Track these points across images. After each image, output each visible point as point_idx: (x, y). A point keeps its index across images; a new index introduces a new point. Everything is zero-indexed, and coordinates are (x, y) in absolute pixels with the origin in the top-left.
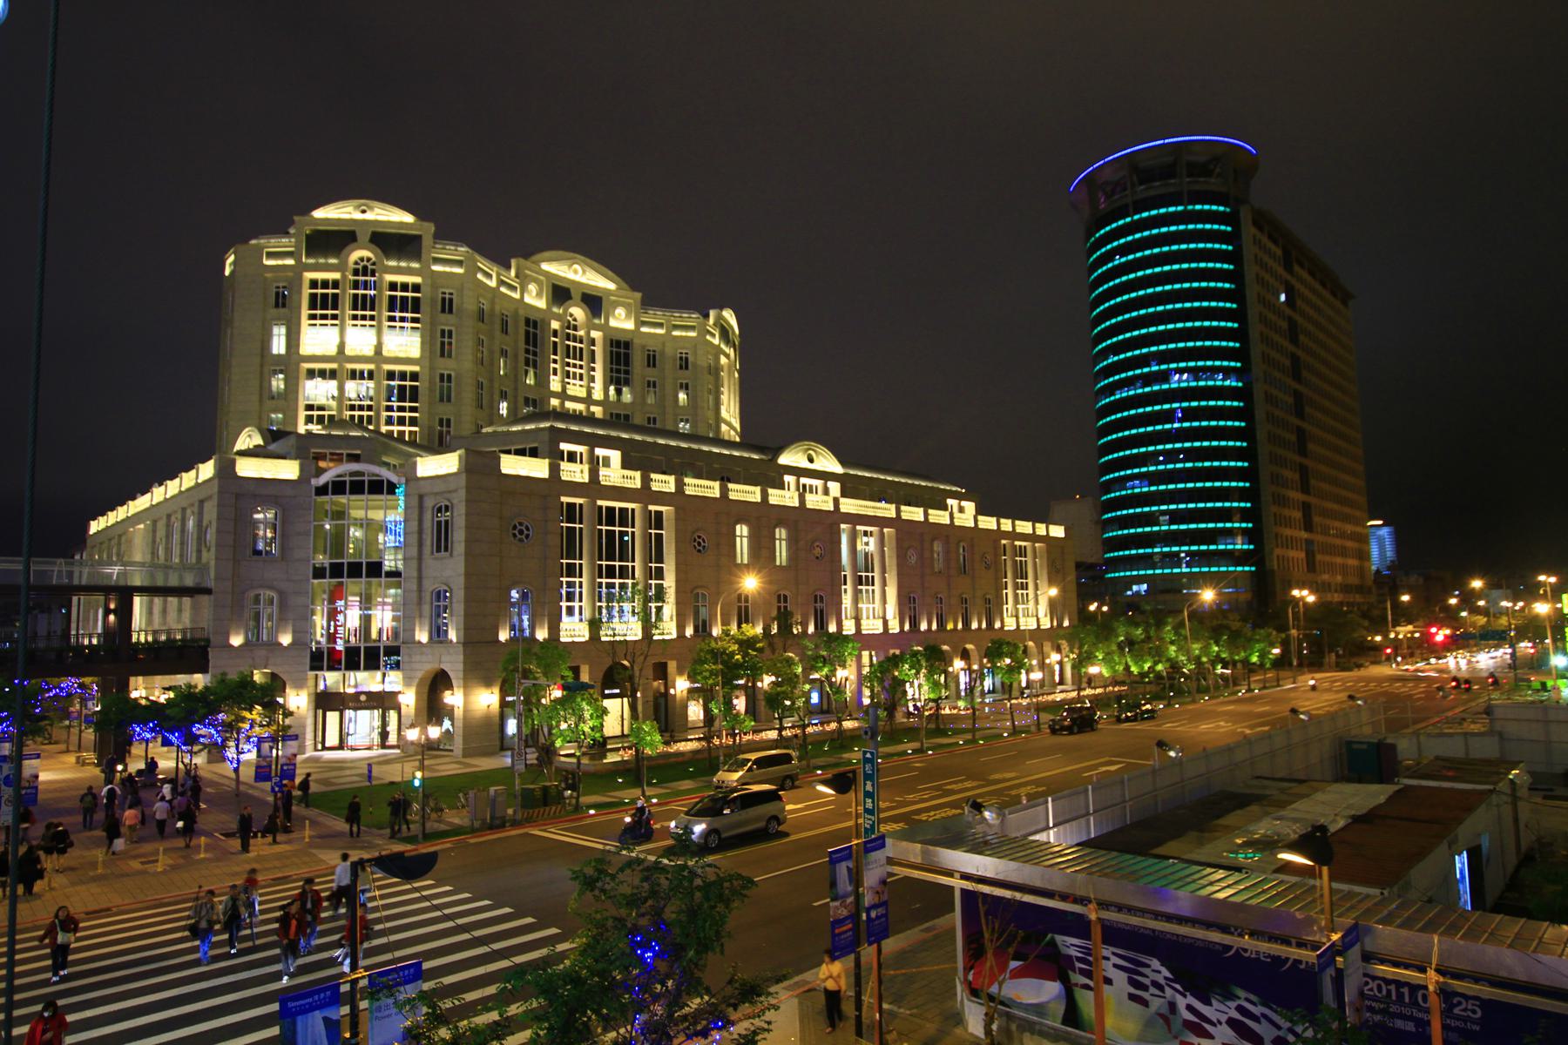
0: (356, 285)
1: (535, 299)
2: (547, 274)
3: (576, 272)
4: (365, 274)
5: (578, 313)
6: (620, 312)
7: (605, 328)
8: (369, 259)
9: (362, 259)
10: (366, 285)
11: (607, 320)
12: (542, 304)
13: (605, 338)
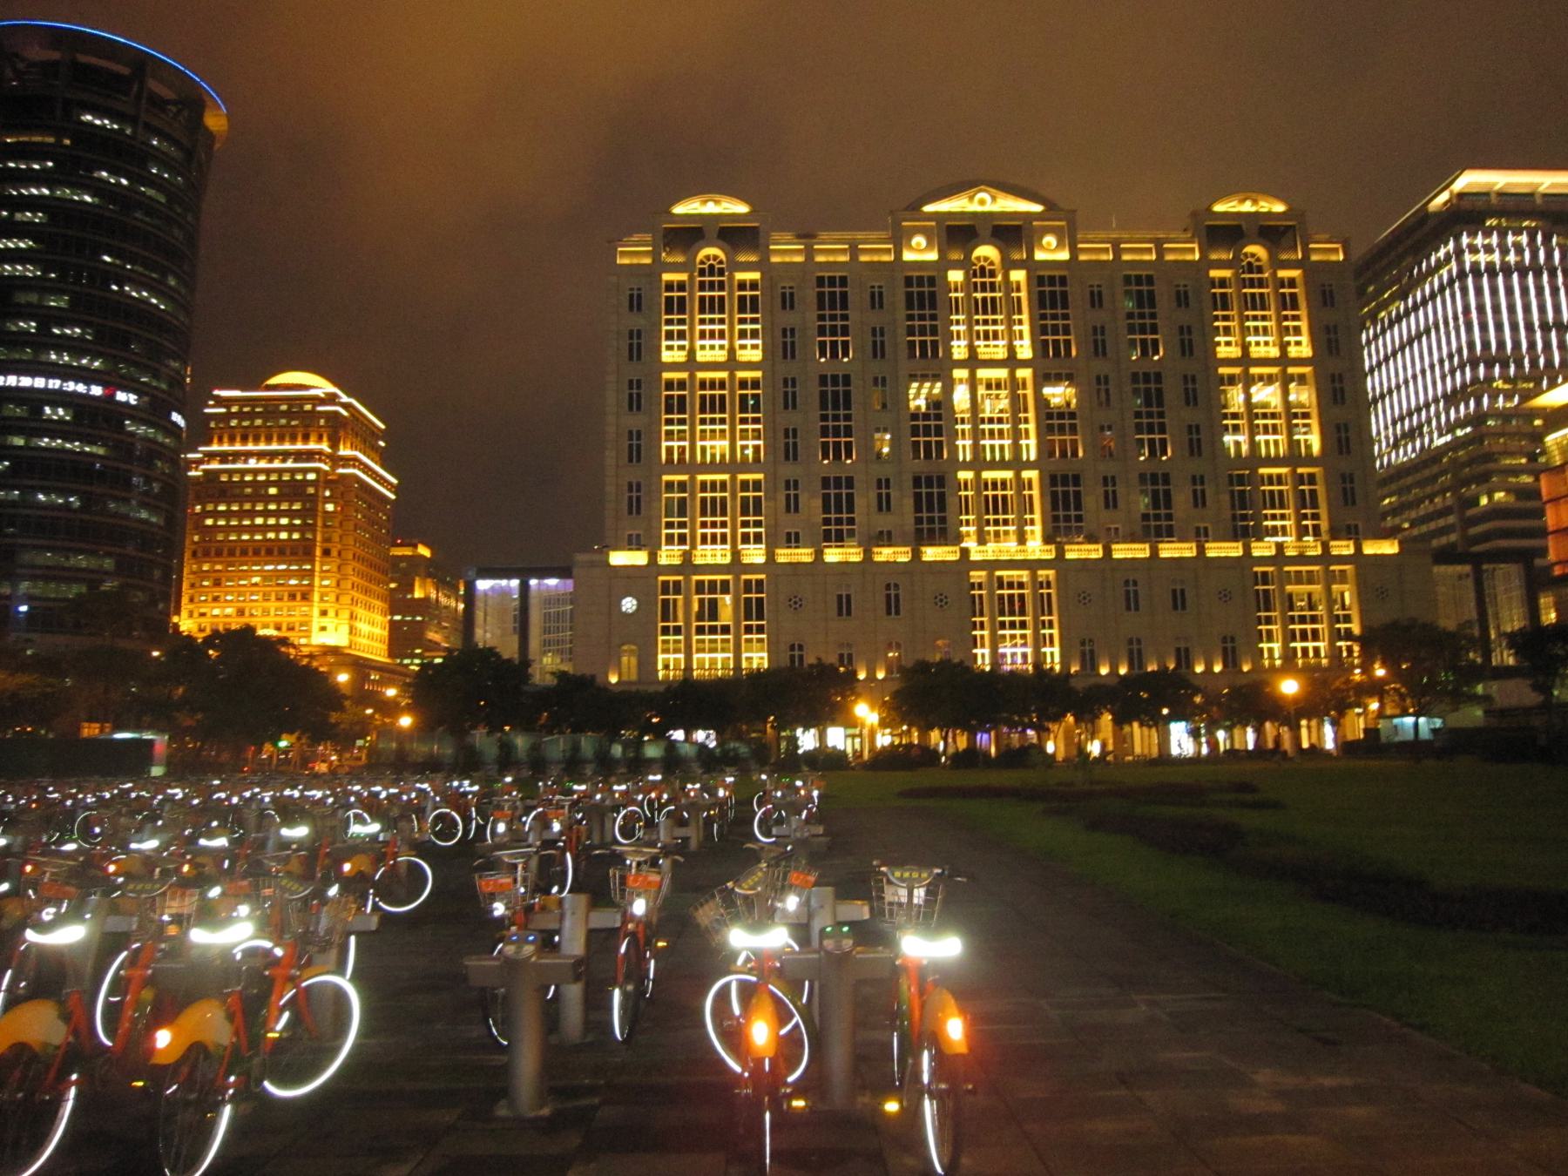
0: (702, 287)
1: (920, 251)
3: (982, 202)
4: (712, 274)
5: (987, 252)
6: (1050, 240)
8: (715, 258)
9: (708, 258)
10: (712, 286)
11: (1031, 253)
12: (933, 256)
13: (1029, 278)
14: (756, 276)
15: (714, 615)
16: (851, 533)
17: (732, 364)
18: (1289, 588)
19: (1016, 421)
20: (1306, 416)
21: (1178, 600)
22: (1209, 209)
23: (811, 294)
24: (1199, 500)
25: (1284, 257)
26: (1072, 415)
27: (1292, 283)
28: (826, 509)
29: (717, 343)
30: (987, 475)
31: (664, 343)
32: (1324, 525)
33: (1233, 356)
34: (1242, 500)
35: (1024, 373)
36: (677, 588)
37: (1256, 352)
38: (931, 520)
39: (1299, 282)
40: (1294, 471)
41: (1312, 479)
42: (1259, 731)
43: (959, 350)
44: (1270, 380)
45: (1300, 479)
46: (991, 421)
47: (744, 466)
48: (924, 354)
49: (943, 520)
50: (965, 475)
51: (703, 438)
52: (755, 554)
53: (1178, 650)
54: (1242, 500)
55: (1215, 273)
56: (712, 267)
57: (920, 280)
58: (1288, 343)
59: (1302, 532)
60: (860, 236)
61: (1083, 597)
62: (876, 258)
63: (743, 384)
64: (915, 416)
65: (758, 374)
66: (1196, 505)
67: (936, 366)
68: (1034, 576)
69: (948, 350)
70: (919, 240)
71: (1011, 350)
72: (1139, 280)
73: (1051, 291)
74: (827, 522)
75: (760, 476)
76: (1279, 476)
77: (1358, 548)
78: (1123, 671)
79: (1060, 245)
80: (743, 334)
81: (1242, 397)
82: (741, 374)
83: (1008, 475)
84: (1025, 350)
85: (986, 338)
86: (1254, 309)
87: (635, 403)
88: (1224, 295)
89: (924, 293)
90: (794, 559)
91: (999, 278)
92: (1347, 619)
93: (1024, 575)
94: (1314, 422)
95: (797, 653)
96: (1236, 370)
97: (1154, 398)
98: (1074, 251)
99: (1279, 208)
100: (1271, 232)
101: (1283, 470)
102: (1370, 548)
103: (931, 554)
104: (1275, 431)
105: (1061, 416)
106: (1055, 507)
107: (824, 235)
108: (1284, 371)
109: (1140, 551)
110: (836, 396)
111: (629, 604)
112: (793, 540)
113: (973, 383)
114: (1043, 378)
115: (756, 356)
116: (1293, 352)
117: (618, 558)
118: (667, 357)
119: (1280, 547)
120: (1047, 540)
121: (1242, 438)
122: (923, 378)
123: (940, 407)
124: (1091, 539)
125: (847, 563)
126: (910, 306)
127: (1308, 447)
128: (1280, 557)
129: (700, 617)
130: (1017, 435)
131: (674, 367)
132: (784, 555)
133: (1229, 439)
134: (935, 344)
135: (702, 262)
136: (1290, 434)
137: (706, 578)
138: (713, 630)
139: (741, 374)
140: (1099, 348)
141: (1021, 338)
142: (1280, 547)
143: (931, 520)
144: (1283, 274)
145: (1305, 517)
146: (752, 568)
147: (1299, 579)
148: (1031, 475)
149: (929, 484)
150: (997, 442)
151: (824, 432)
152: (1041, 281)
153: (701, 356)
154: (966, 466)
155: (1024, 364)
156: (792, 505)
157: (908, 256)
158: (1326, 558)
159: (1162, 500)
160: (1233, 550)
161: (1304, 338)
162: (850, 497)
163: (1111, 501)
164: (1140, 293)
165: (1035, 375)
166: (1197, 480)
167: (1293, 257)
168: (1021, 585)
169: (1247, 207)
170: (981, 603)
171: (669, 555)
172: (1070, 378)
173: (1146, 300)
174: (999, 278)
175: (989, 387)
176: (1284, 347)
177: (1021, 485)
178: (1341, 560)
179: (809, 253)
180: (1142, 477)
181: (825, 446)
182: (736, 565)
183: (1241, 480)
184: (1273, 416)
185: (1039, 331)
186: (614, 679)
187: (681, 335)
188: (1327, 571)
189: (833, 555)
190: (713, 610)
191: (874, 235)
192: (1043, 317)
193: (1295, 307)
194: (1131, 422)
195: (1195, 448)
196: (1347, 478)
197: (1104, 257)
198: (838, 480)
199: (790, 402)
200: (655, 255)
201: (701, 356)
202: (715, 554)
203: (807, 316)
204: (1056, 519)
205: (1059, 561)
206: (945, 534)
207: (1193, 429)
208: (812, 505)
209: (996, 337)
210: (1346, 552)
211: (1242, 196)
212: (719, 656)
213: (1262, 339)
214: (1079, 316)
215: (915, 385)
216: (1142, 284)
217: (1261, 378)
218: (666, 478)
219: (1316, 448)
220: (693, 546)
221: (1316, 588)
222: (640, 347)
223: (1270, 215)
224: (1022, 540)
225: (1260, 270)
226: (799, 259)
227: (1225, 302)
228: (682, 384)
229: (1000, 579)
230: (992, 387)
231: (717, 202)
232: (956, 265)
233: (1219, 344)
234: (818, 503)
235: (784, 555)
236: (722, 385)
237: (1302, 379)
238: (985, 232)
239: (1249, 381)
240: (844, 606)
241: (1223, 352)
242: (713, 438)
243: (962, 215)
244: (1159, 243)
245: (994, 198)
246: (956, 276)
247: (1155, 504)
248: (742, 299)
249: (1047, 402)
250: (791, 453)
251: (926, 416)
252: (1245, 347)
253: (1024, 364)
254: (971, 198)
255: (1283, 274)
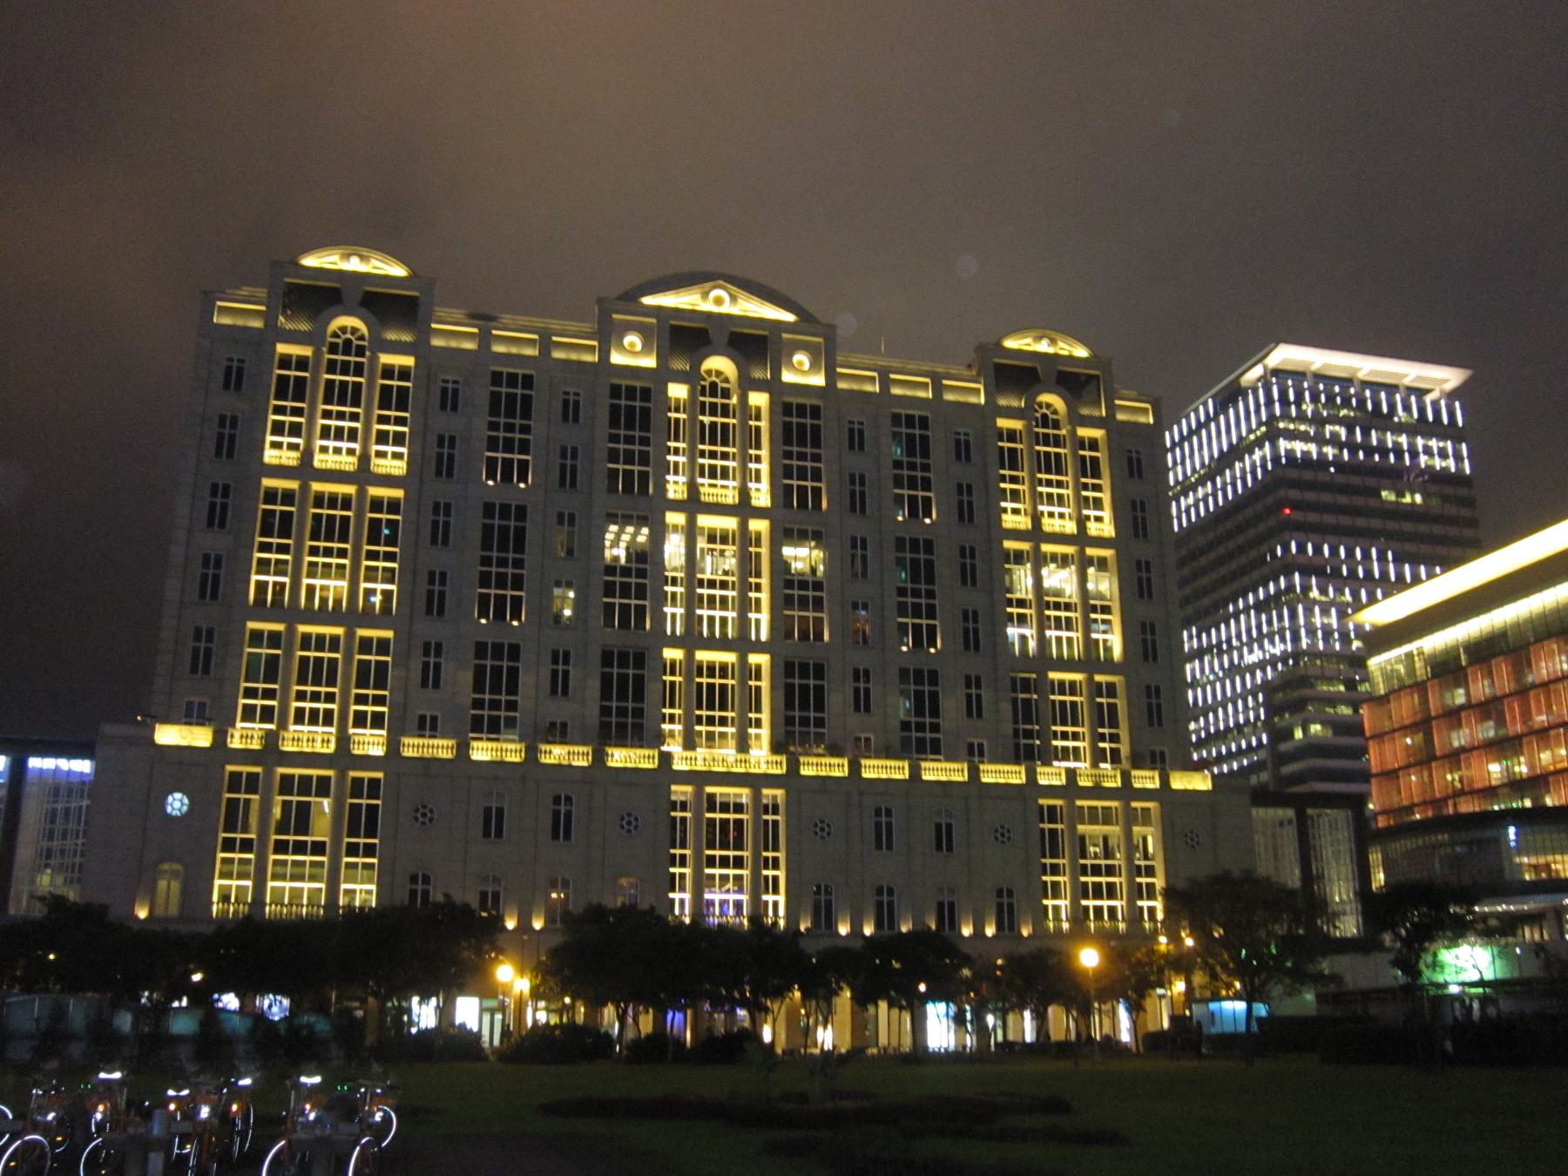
1: (633, 354)
2: (658, 311)
3: (719, 301)
4: (347, 352)
5: (720, 364)
6: (801, 358)
7: (773, 386)
8: (354, 330)
9: (344, 329)
11: (777, 373)
12: (650, 362)
13: (772, 402)
14: (408, 361)
15: (303, 826)
16: (511, 723)
17: (363, 475)
18: (1081, 828)
19: (745, 587)
20: (1106, 610)
21: (943, 838)
22: (998, 344)
23: (481, 394)
24: (974, 708)
25: (1085, 411)
26: (818, 586)
27: (1093, 445)
28: (478, 686)
29: (345, 445)
30: (703, 656)
31: (269, 438)
32: (1124, 748)
33: (1022, 527)
34: (1026, 712)
35: (759, 526)
36: (252, 783)
37: (1049, 525)
38: (622, 712)
39: (1102, 445)
40: (1090, 679)
41: (1111, 690)
42: (1040, 1018)
43: (676, 487)
44: (1064, 561)
45: (1097, 689)
46: (712, 584)
47: (369, 617)
48: (628, 487)
49: (639, 713)
50: (672, 654)
51: (311, 575)
52: (371, 743)
53: (940, 905)
54: (1026, 712)
55: (1003, 423)
56: (348, 342)
57: (631, 392)
58: (1088, 518)
59: (1098, 757)
60: (555, 324)
61: (822, 827)
62: (574, 356)
63: (377, 505)
64: (611, 569)
65: (399, 493)
66: (970, 714)
67: (646, 507)
68: (757, 796)
69: (662, 486)
70: (633, 340)
71: (744, 493)
72: (910, 420)
73: (800, 423)
74: (478, 704)
75: (389, 634)
76: (1073, 684)
77: (1165, 781)
78: (868, 930)
79: (814, 366)
80: (382, 438)
81: (1030, 581)
82: (374, 491)
83: (730, 658)
84: (762, 496)
85: (713, 475)
86: (1048, 471)
87: (217, 518)
88: (1012, 451)
89: (634, 406)
90: (427, 753)
91: (734, 400)
92: (1150, 871)
93: (743, 794)
94: (1115, 618)
95: (420, 887)
96: (1025, 546)
97: (923, 572)
98: (831, 376)
99: (1081, 352)
100: (1071, 380)
101: (1078, 677)
102: (1179, 782)
103: (619, 757)
104: (1069, 628)
105: (803, 585)
106: (789, 704)
107: (506, 319)
108: (1082, 552)
109: (897, 770)
110: (505, 533)
111: (177, 803)
112: (427, 727)
113: (691, 532)
114: (785, 533)
115: (398, 468)
116: (1093, 529)
117: (168, 735)
118: (270, 456)
119: (1071, 774)
120: (776, 748)
121: (1029, 632)
122: (625, 520)
123: (646, 560)
124: (834, 751)
125: (502, 763)
126: (614, 423)
127: (1108, 649)
128: (1071, 788)
129: (282, 828)
130: (745, 605)
131: (281, 471)
132: (413, 747)
133: (1013, 632)
134: (644, 477)
135: (335, 335)
136: (1087, 632)
137: (297, 771)
138: (300, 848)
139: (374, 491)
140: (857, 503)
141: (758, 480)
142: (1071, 774)
143: (622, 712)
144: (1084, 432)
145: (1102, 738)
146: (367, 762)
147: (1094, 816)
148: (760, 659)
149: (623, 663)
150: (717, 614)
151: (485, 580)
152: (787, 409)
153: (320, 461)
154: (674, 642)
155: (760, 513)
156: (431, 678)
157: (616, 358)
158: (1127, 792)
159: (927, 705)
160: (1013, 775)
161: (1107, 514)
162: (514, 672)
163: (862, 702)
164: (911, 438)
165: (773, 529)
166: (972, 681)
167: (1096, 413)
168: (739, 808)
169: (1043, 347)
170: (684, 831)
171: (245, 735)
172: (818, 537)
173: (918, 447)
174: (734, 400)
175: (712, 539)
176: (1082, 522)
177: (748, 672)
178: (1145, 794)
179: (485, 339)
180: (904, 673)
181: (484, 599)
182: (344, 756)
183: (1026, 685)
184: (1068, 607)
185: (781, 472)
186: (142, 914)
187: (295, 430)
188: (1127, 808)
189: (482, 751)
190: (301, 818)
191: (572, 326)
192: (788, 455)
193: (1096, 474)
194: (893, 600)
195: (971, 641)
196: (1152, 692)
197: (868, 388)
198: (498, 648)
199: (440, 535)
200: (269, 317)
201: (320, 461)
202: (316, 739)
203: (475, 422)
204: (789, 721)
205: (790, 781)
206: (642, 733)
207: (970, 616)
208: (459, 678)
209: (725, 475)
210: (1150, 785)
211: (1039, 332)
212: (306, 886)
213: (1056, 510)
214: (832, 454)
215: (614, 528)
216: (914, 428)
217: (1054, 558)
218: (252, 625)
219: (1117, 652)
220: (283, 725)
221: (1114, 830)
222: (234, 443)
223: (1071, 358)
224: (743, 746)
225: (1056, 425)
226: (470, 345)
227: (1013, 460)
228: (288, 497)
229: (711, 797)
230: (714, 539)
231: (363, 258)
232: (680, 377)
233: (1005, 510)
234: (468, 677)
235: (413, 747)
236: (346, 503)
237: (1102, 564)
238: (720, 338)
239: (1039, 560)
240: (493, 824)
241: (1009, 521)
242: (326, 576)
243: (693, 314)
244: (937, 379)
245: (733, 298)
246: (678, 391)
247: (919, 711)
248: (386, 390)
249: (787, 566)
250: (435, 605)
251: (625, 571)
252: (1036, 518)
253: (760, 513)
254: (705, 295)
255: (1084, 432)
